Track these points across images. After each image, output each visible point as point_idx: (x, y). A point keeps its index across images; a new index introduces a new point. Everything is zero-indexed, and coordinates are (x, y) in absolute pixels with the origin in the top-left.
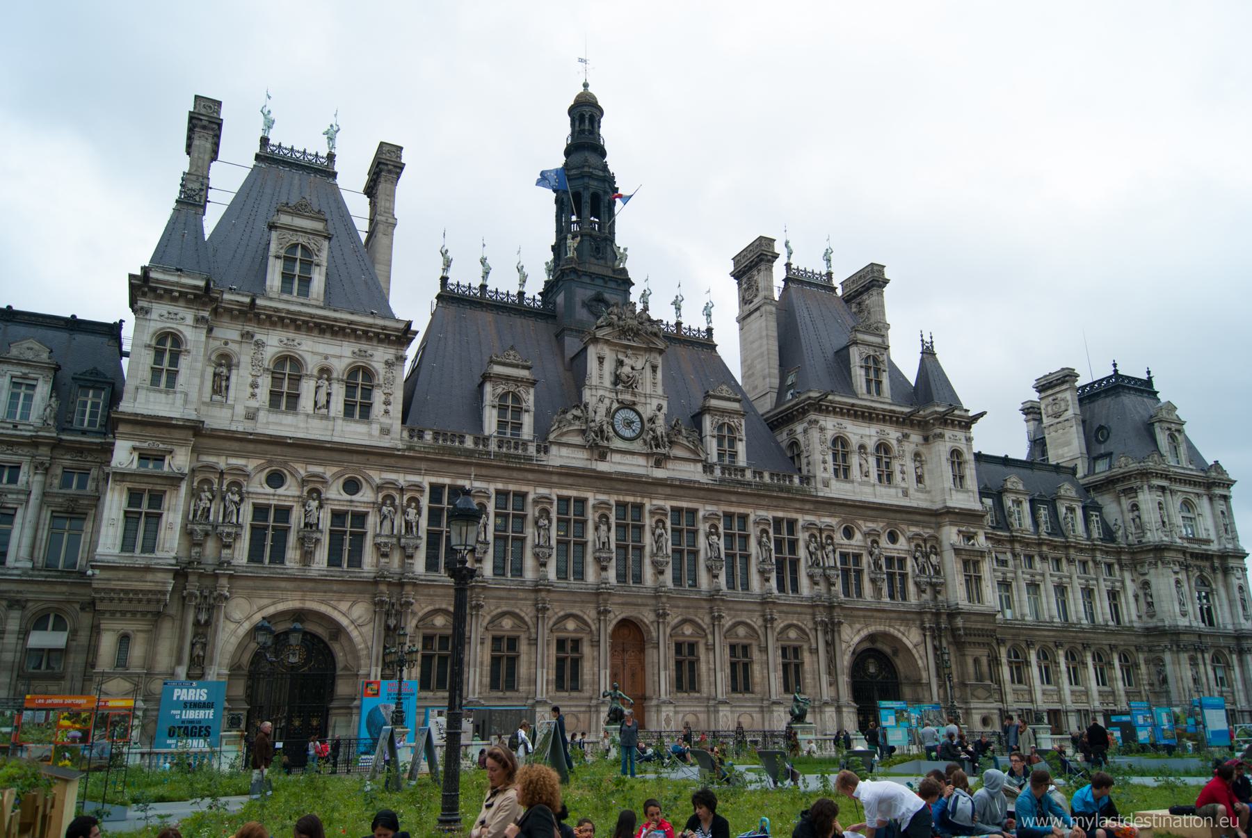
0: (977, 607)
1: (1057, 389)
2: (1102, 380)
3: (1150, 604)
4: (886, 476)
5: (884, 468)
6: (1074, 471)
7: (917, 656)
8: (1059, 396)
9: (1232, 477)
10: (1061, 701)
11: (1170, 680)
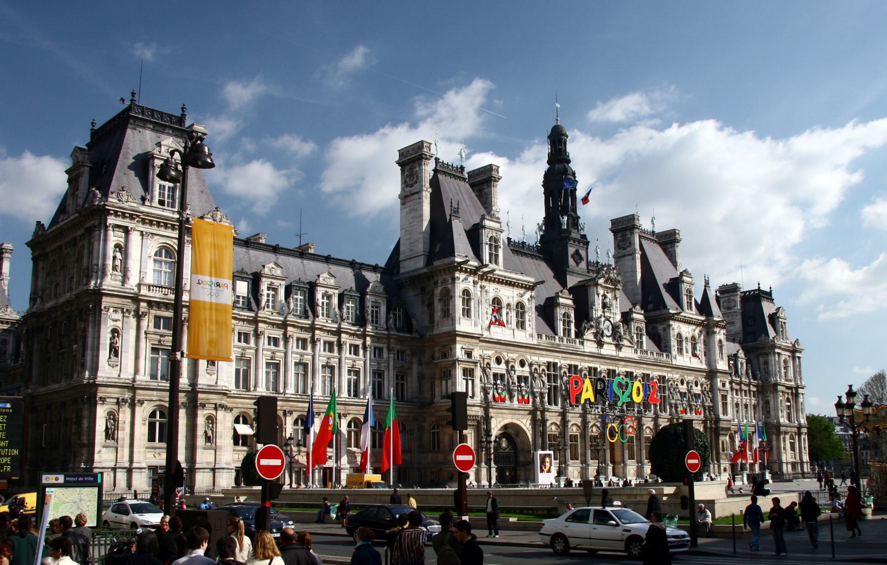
0: (725, 417)
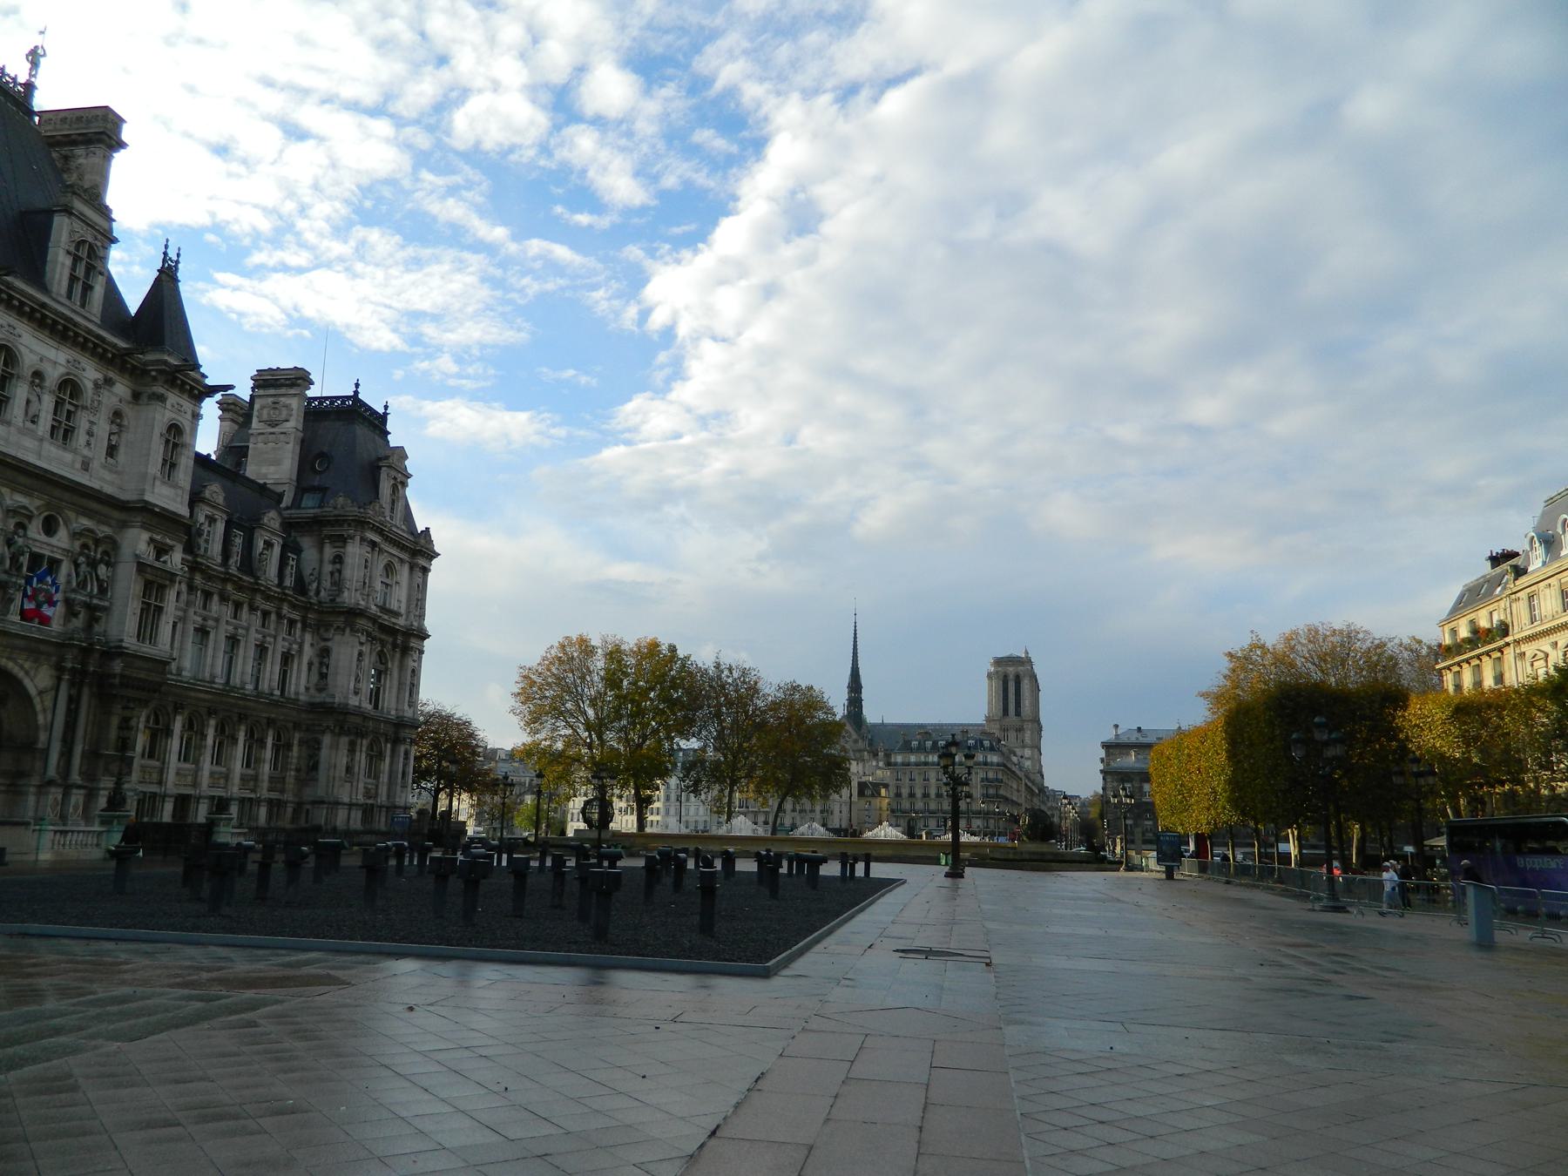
0: (146, 649)
1: (283, 391)
2: (338, 398)
3: (323, 676)
4: (63, 432)
5: (63, 419)
6: (280, 496)
7: (38, 707)
8: (282, 399)
9: (437, 549)
10: (195, 784)
11: (323, 766)
